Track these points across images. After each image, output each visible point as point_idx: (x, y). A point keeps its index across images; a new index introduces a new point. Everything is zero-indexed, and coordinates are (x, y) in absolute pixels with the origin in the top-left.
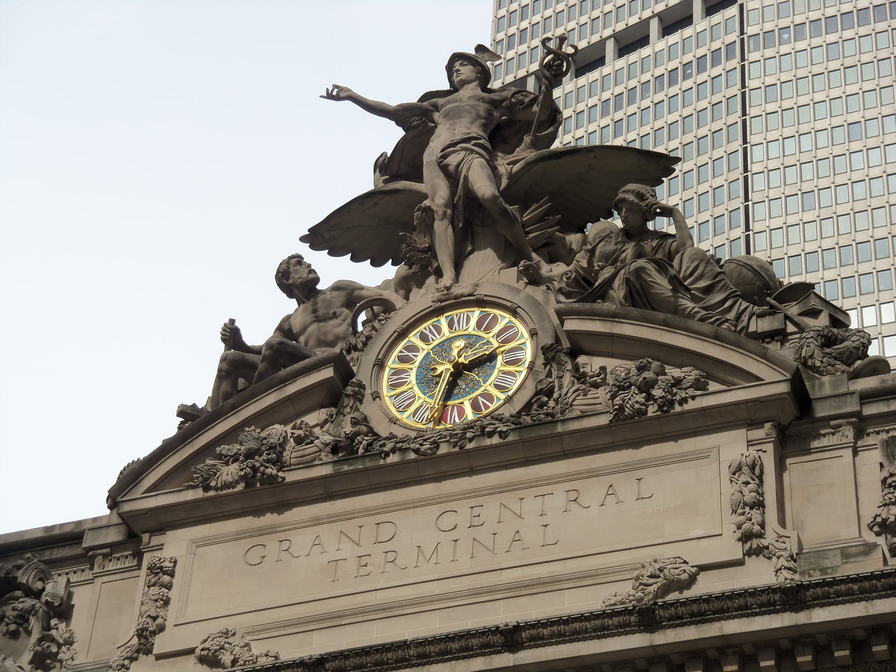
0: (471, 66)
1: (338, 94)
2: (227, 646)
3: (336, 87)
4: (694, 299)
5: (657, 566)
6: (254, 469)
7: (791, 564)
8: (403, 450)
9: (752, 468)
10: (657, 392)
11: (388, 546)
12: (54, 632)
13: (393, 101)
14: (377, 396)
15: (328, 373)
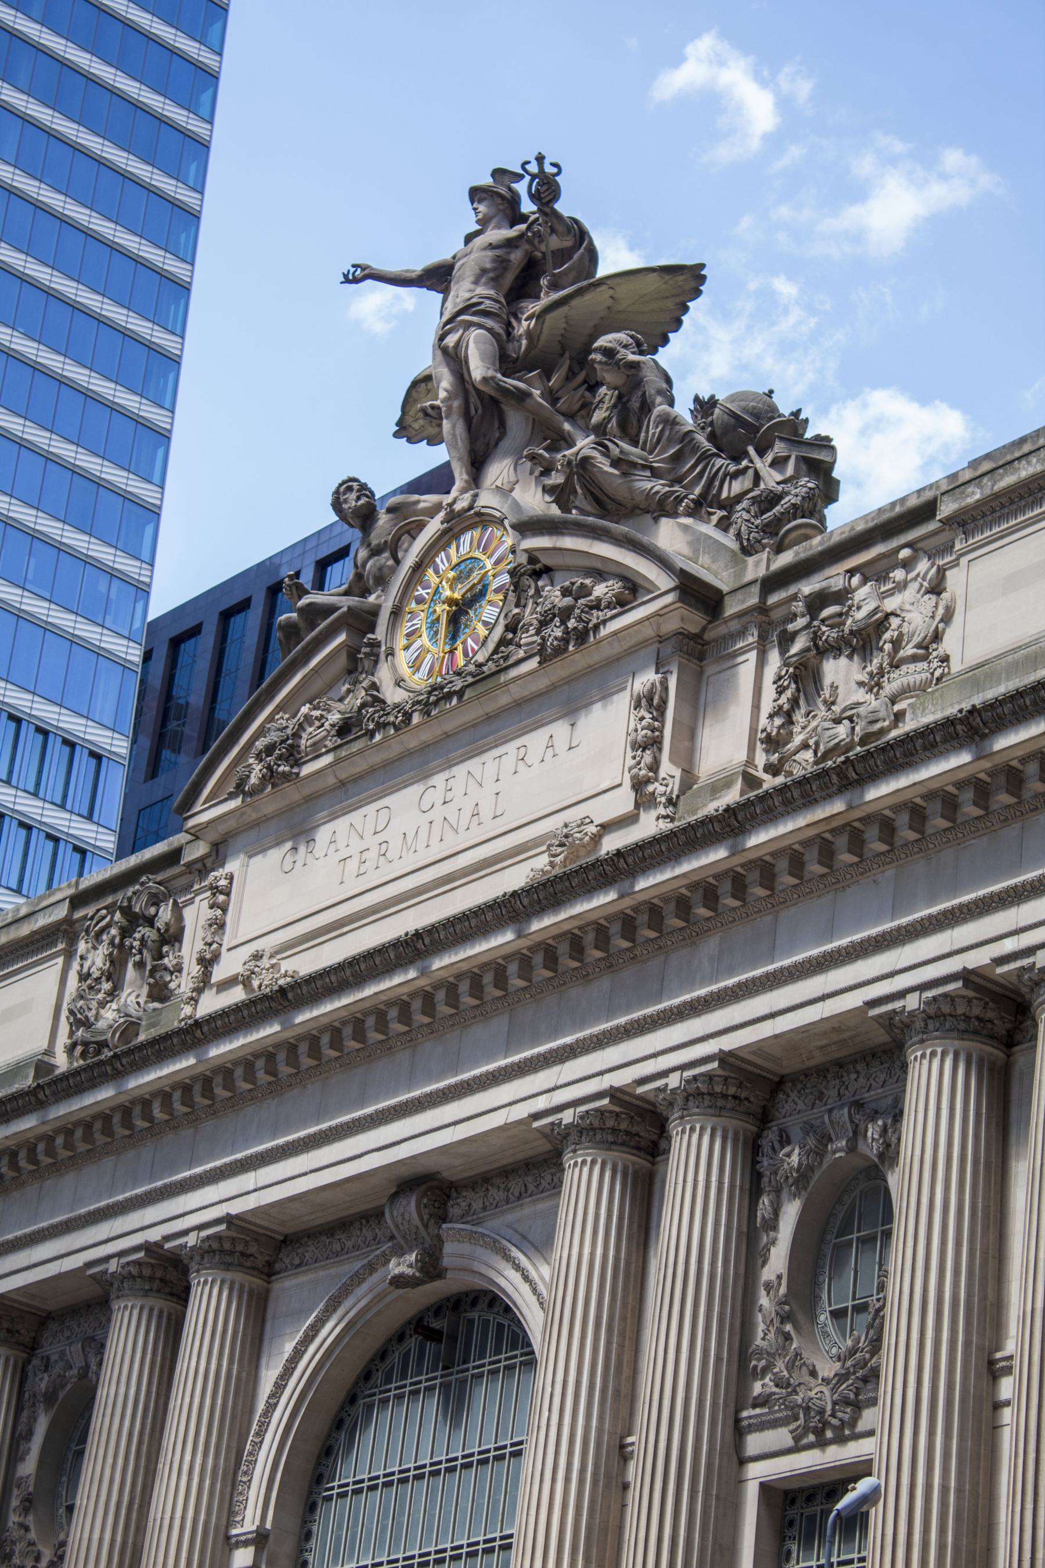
0: (495, 197)
1: (360, 275)
2: (257, 969)
3: (353, 266)
4: (655, 474)
5: (565, 830)
6: (269, 768)
7: (670, 810)
8: (385, 725)
9: (650, 700)
10: (572, 623)
11: (381, 837)
12: (166, 961)
13: (417, 265)
14: (391, 653)
15: (342, 638)
